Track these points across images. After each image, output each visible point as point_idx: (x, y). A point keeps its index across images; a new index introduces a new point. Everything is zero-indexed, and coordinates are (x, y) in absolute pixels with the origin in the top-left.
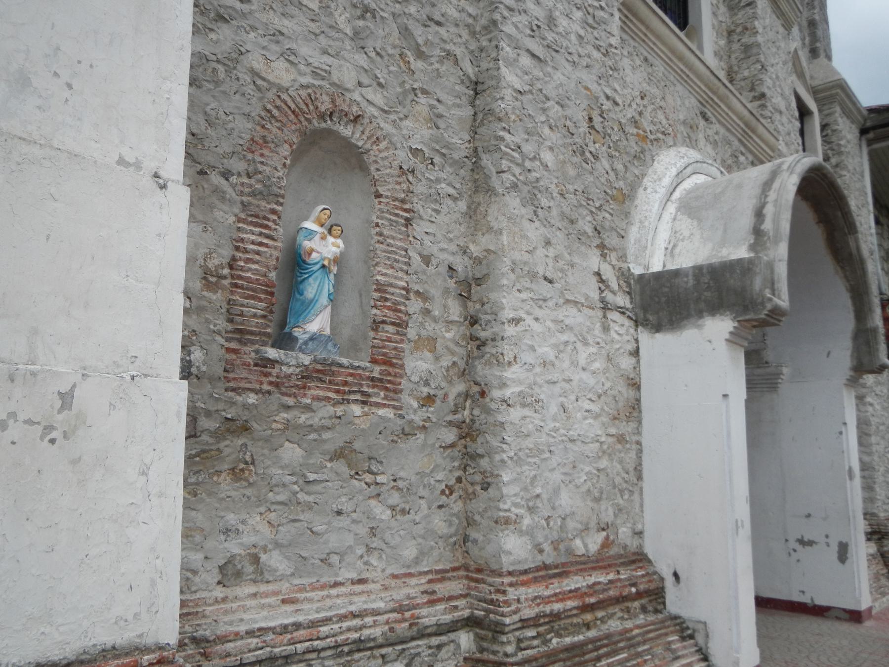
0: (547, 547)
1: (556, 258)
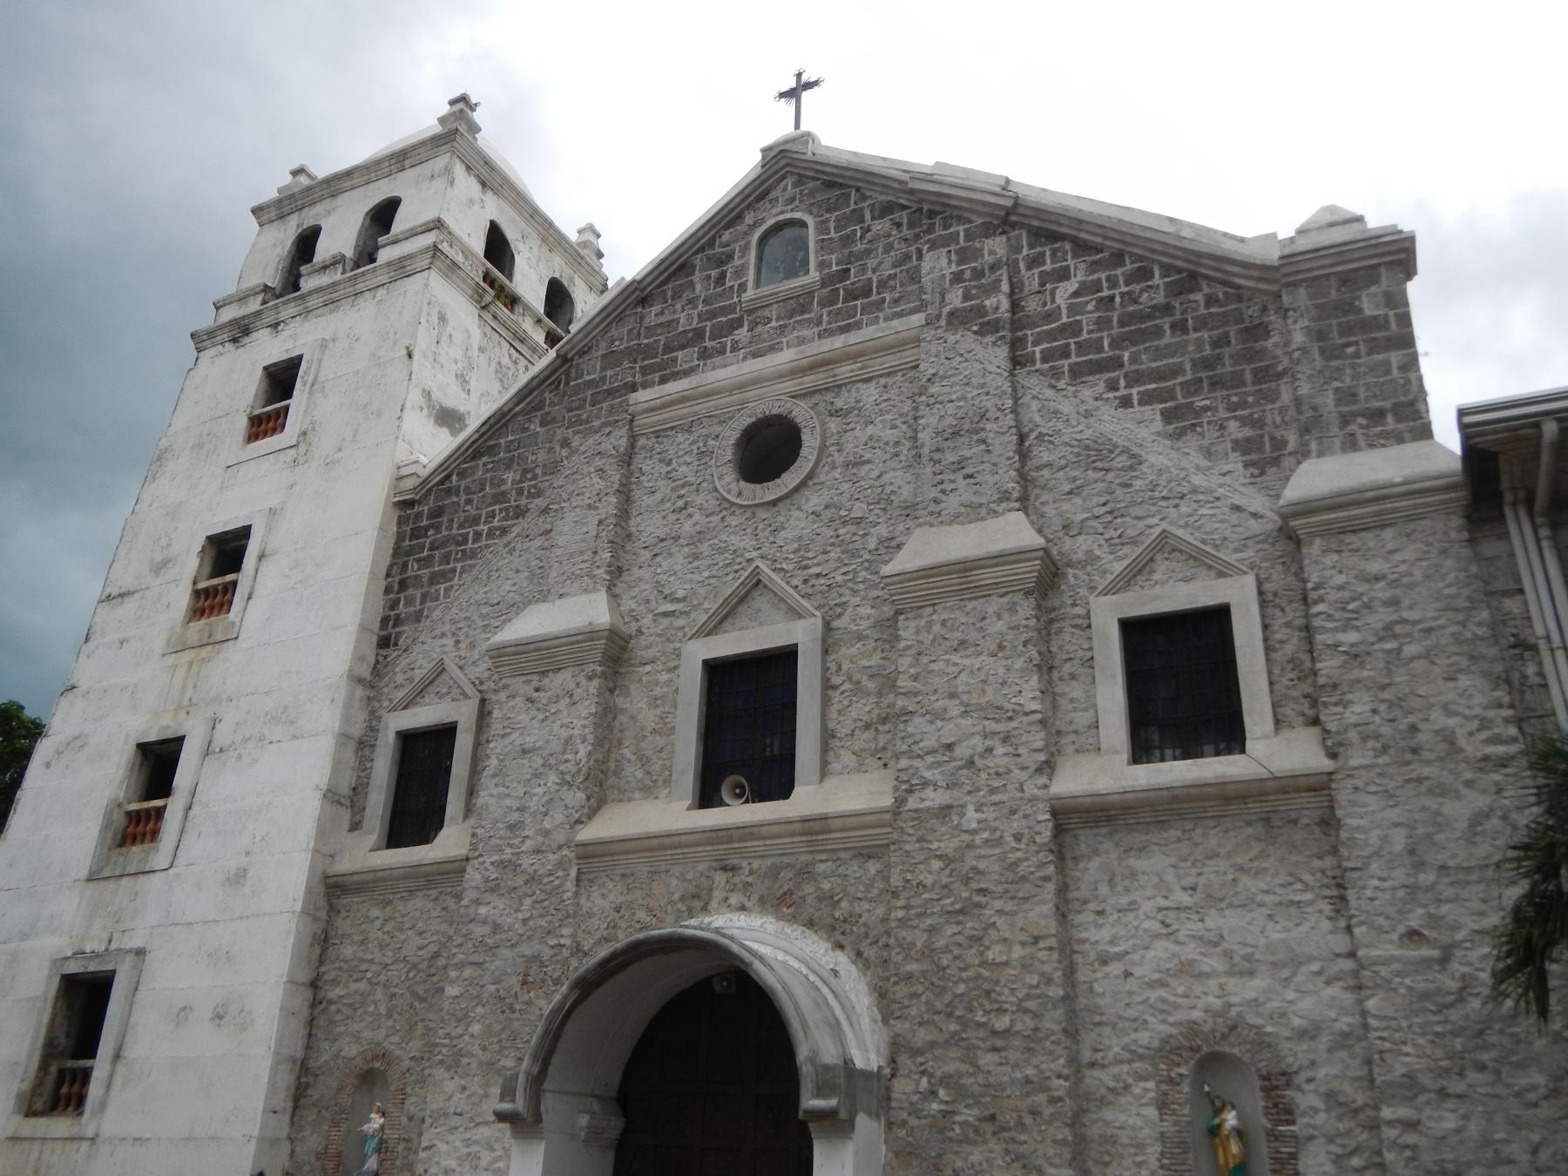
1: (470, 1096)
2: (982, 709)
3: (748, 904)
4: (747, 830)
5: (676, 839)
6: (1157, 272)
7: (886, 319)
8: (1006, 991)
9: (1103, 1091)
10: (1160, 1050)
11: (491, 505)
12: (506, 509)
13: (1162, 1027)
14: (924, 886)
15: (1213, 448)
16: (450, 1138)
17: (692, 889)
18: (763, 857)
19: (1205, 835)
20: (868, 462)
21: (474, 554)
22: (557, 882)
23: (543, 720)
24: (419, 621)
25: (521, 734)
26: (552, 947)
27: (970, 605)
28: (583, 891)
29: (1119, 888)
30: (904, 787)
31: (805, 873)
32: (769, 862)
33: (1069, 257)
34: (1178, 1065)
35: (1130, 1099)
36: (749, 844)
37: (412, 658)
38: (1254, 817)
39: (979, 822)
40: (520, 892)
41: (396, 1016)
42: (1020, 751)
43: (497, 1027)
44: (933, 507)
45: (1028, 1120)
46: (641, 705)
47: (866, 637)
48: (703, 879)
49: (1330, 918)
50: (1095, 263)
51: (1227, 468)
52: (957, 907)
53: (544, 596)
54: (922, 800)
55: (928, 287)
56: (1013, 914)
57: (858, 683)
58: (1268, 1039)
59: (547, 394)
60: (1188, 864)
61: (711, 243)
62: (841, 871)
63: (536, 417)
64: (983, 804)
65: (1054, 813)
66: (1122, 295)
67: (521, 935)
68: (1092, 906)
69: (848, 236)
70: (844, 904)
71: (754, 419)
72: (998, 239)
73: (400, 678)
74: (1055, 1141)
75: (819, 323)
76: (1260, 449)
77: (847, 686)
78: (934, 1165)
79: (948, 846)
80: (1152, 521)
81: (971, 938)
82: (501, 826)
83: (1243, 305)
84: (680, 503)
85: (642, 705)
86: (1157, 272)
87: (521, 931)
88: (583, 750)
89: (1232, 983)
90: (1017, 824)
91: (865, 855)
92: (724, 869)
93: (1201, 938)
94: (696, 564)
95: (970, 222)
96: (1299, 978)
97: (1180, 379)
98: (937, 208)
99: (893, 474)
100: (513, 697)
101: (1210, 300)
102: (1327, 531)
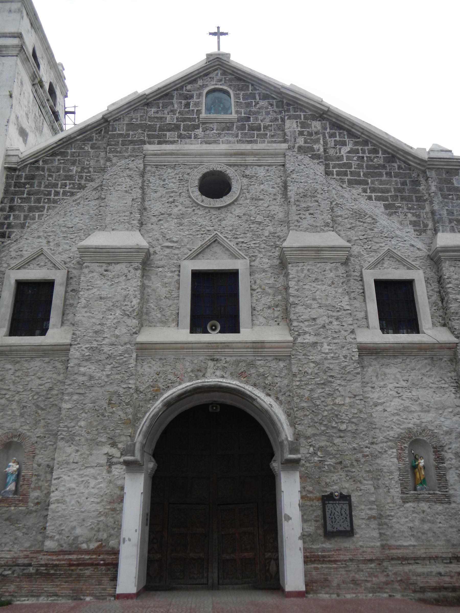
0: (65, 545)
1: (81, 455)
2: (327, 306)
3: (225, 376)
4: (226, 344)
5: (190, 345)
6: (380, 152)
7: (269, 142)
8: (344, 415)
9: (377, 453)
10: (398, 438)
11: (63, 180)
12: (73, 184)
13: (398, 430)
14: (307, 373)
15: (403, 222)
16: (70, 474)
17: (197, 367)
18: (231, 356)
19: (410, 362)
20: (262, 200)
21: (55, 202)
22: (125, 359)
23: (111, 285)
24: (24, 228)
25: (98, 290)
26: (124, 388)
27: (319, 265)
28: (138, 364)
29: (380, 379)
30: (296, 333)
31: (251, 364)
32: (234, 358)
33: (346, 137)
34: (404, 443)
35: (387, 456)
36: (226, 350)
37: (20, 245)
38: (428, 357)
39: (329, 350)
40: (103, 362)
41: (26, 417)
42: (344, 324)
43: (95, 423)
44: (296, 223)
45: (355, 463)
46: (157, 285)
47: (266, 271)
48: (202, 364)
49: (454, 393)
50: (357, 142)
51: (408, 230)
52: (322, 382)
53: (104, 228)
54: (304, 339)
55: (288, 134)
56: (345, 386)
57: (264, 289)
58: (436, 434)
59: (94, 135)
60: (405, 371)
61: (181, 88)
62: (268, 364)
63: (88, 144)
64: (330, 343)
65: (358, 348)
66: (367, 157)
67: (106, 382)
68: (369, 385)
69: (249, 103)
70: (269, 378)
71: (208, 170)
72: (318, 122)
73: (13, 254)
74: (366, 471)
75: (237, 136)
76: (419, 226)
77: (259, 290)
78: (317, 481)
79: (317, 358)
80: (383, 245)
81: (329, 394)
82: (91, 331)
83: (411, 172)
84: (171, 200)
85: (159, 285)
86: (380, 152)
87: (106, 380)
88: (135, 302)
89: (422, 415)
90: (345, 352)
91: (278, 359)
92: (213, 360)
93: (411, 398)
94: (181, 227)
95: (306, 112)
96: (445, 414)
97: (390, 194)
98: (291, 103)
99: (274, 207)
100: (92, 272)
101: (400, 167)
102: (451, 259)
